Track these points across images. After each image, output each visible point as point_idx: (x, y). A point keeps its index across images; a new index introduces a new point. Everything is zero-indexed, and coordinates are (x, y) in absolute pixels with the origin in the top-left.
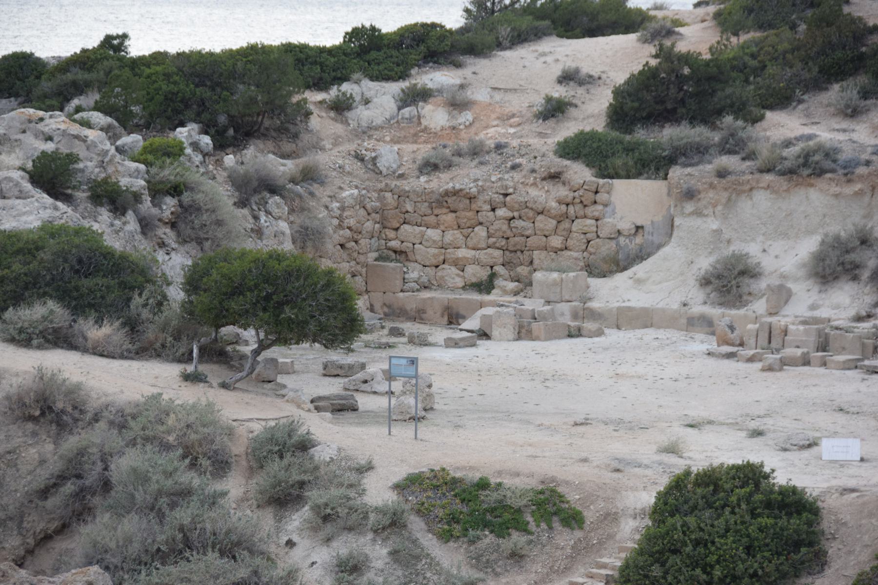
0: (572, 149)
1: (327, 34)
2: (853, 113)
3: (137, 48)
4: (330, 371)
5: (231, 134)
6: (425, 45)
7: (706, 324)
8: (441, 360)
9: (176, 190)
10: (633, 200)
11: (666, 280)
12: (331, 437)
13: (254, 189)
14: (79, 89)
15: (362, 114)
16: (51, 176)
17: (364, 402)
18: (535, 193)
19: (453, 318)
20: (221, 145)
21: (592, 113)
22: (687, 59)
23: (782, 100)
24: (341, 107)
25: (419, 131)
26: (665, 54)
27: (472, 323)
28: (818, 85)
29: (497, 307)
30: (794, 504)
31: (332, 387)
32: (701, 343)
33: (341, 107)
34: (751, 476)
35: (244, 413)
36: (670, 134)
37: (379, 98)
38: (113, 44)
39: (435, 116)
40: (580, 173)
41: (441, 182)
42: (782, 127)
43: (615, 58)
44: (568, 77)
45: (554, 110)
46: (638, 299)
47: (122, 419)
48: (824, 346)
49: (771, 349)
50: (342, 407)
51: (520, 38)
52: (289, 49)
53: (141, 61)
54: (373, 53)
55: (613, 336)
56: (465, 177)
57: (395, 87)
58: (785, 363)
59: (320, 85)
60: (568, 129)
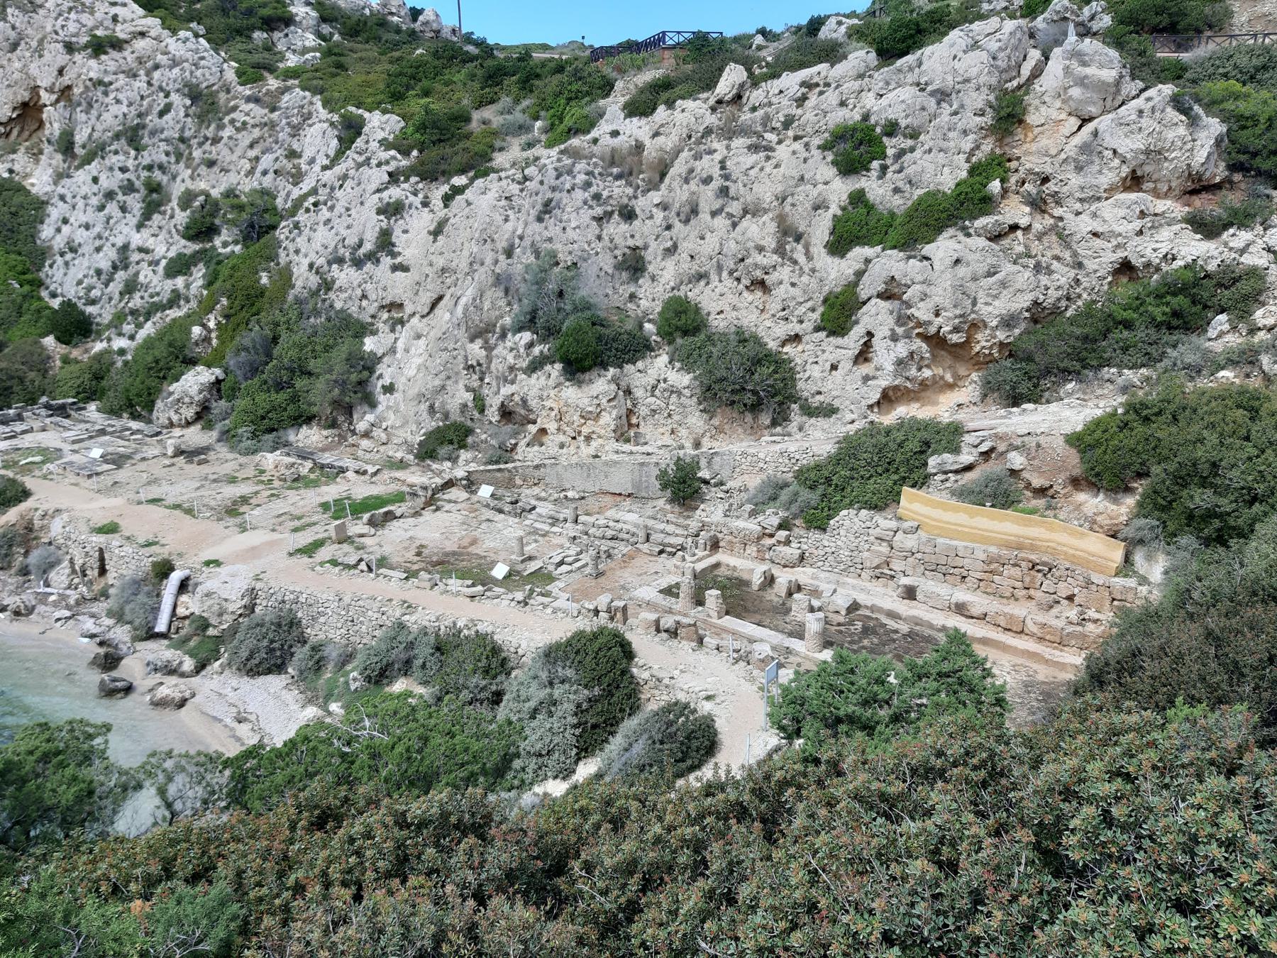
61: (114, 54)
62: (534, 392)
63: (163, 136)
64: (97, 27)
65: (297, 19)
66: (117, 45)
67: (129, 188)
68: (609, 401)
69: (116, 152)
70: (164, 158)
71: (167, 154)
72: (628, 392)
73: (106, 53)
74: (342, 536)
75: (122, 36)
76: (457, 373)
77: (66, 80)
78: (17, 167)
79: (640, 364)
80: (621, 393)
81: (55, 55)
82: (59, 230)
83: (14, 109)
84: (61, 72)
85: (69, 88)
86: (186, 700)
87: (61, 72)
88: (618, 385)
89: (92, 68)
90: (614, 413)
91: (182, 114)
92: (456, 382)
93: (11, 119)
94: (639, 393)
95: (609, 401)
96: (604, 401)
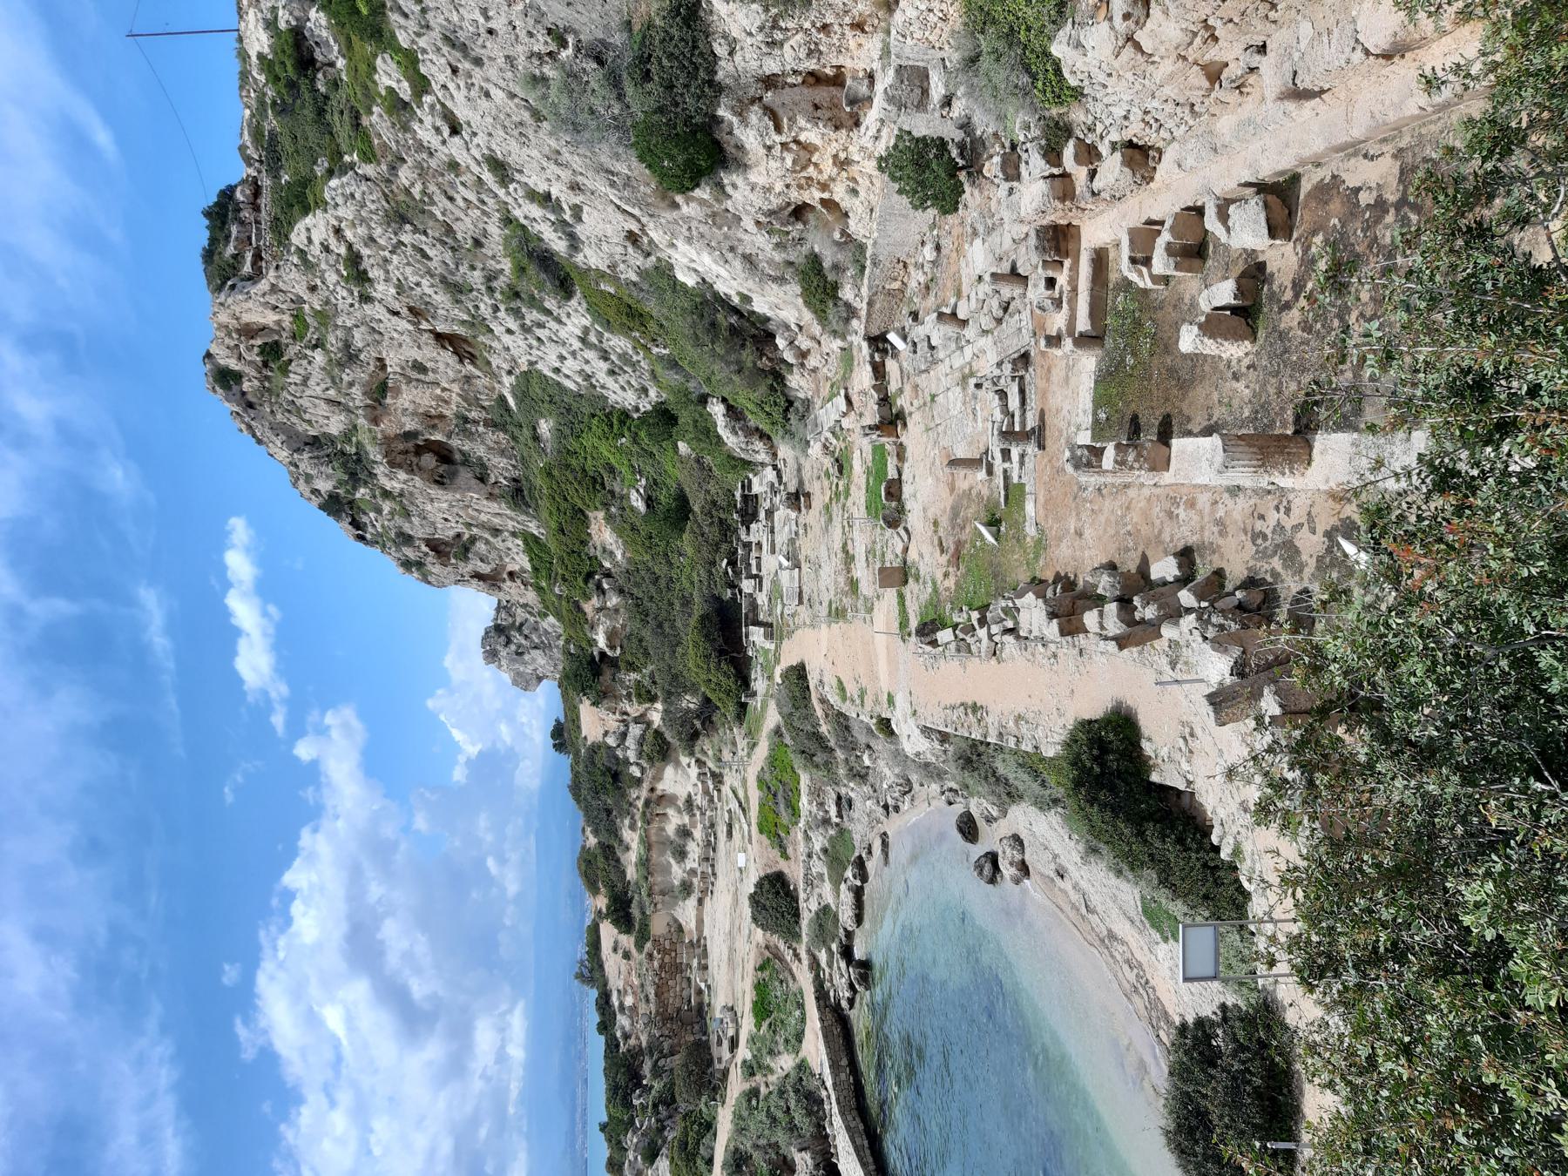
0: (640, 946)
1: (598, 1043)
2: (628, 848)
3: (605, 1119)
4: (720, 1043)
5: (635, 1078)
6: (604, 1002)
7: (700, 902)
8: (719, 1001)
9: (655, 1106)
10: (658, 926)
11: (686, 912)
12: (744, 1052)
13: (657, 1072)
14: (619, 1142)
15: (627, 1028)
16: (651, 1155)
17: (731, 1032)
18: (656, 964)
19: (700, 992)
20: (639, 1085)
21: (627, 941)
22: (608, 908)
23: (624, 873)
24: (626, 1037)
25: (634, 1008)
26: (607, 916)
27: (703, 985)
28: (618, 861)
29: (696, 977)
30: (759, 885)
31: (726, 1044)
32: (707, 900)
33: (626, 1037)
34: (753, 899)
35: (736, 1086)
36: (635, 911)
37: (623, 1021)
38: (603, 1128)
39: (629, 1001)
40: (648, 945)
41: (652, 997)
42: (631, 873)
43: (608, 931)
44: (615, 950)
45: (627, 956)
46: (693, 925)
47: (740, 1130)
48: (707, 859)
49: (709, 879)
50: (734, 1043)
51: (601, 966)
52: (606, 1057)
53: (610, 1116)
54: (606, 1026)
55: (706, 933)
56: (651, 991)
57: (619, 1017)
58: (714, 874)
59: (618, 1046)
60: (634, 951)
61: (366, 264)
62: (757, 200)
63: (452, 266)
64: (338, 271)
65: (294, 23)
66: (354, 259)
67: (516, 313)
68: (778, 129)
69: (477, 307)
70: (477, 273)
71: (473, 268)
72: (770, 82)
73: (365, 272)
74: (898, 577)
75: (343, 250)
76: (726, 237)
77: (404, 312)
78: (506, 366)
79: (720, 49)
80: (769, 96)
81: (376, 311)
82: (568, 377)
83: (444, 347)
84: (396, 314)
85: (411, 309)
86: (1023, 862)
87: (396, 314)
88: (753, 101)
89: (383, 290)
90: (802, 122)
91: (424, 238)
92: (739, 240)
93: (455, 352)
94: (771, 66)
95: (778, 129)
96: (778, 139)
